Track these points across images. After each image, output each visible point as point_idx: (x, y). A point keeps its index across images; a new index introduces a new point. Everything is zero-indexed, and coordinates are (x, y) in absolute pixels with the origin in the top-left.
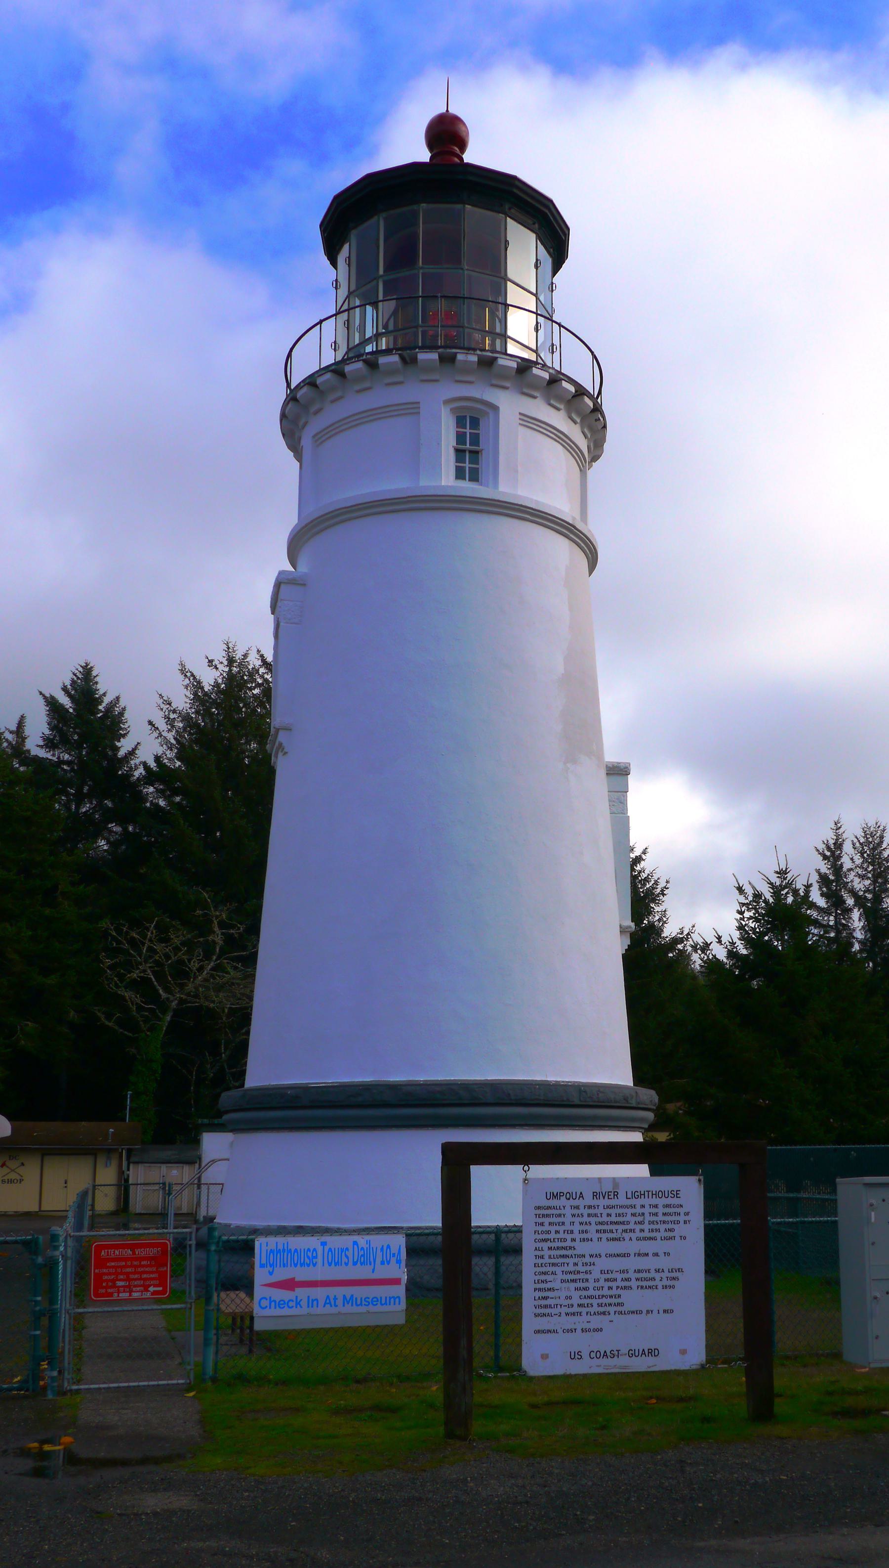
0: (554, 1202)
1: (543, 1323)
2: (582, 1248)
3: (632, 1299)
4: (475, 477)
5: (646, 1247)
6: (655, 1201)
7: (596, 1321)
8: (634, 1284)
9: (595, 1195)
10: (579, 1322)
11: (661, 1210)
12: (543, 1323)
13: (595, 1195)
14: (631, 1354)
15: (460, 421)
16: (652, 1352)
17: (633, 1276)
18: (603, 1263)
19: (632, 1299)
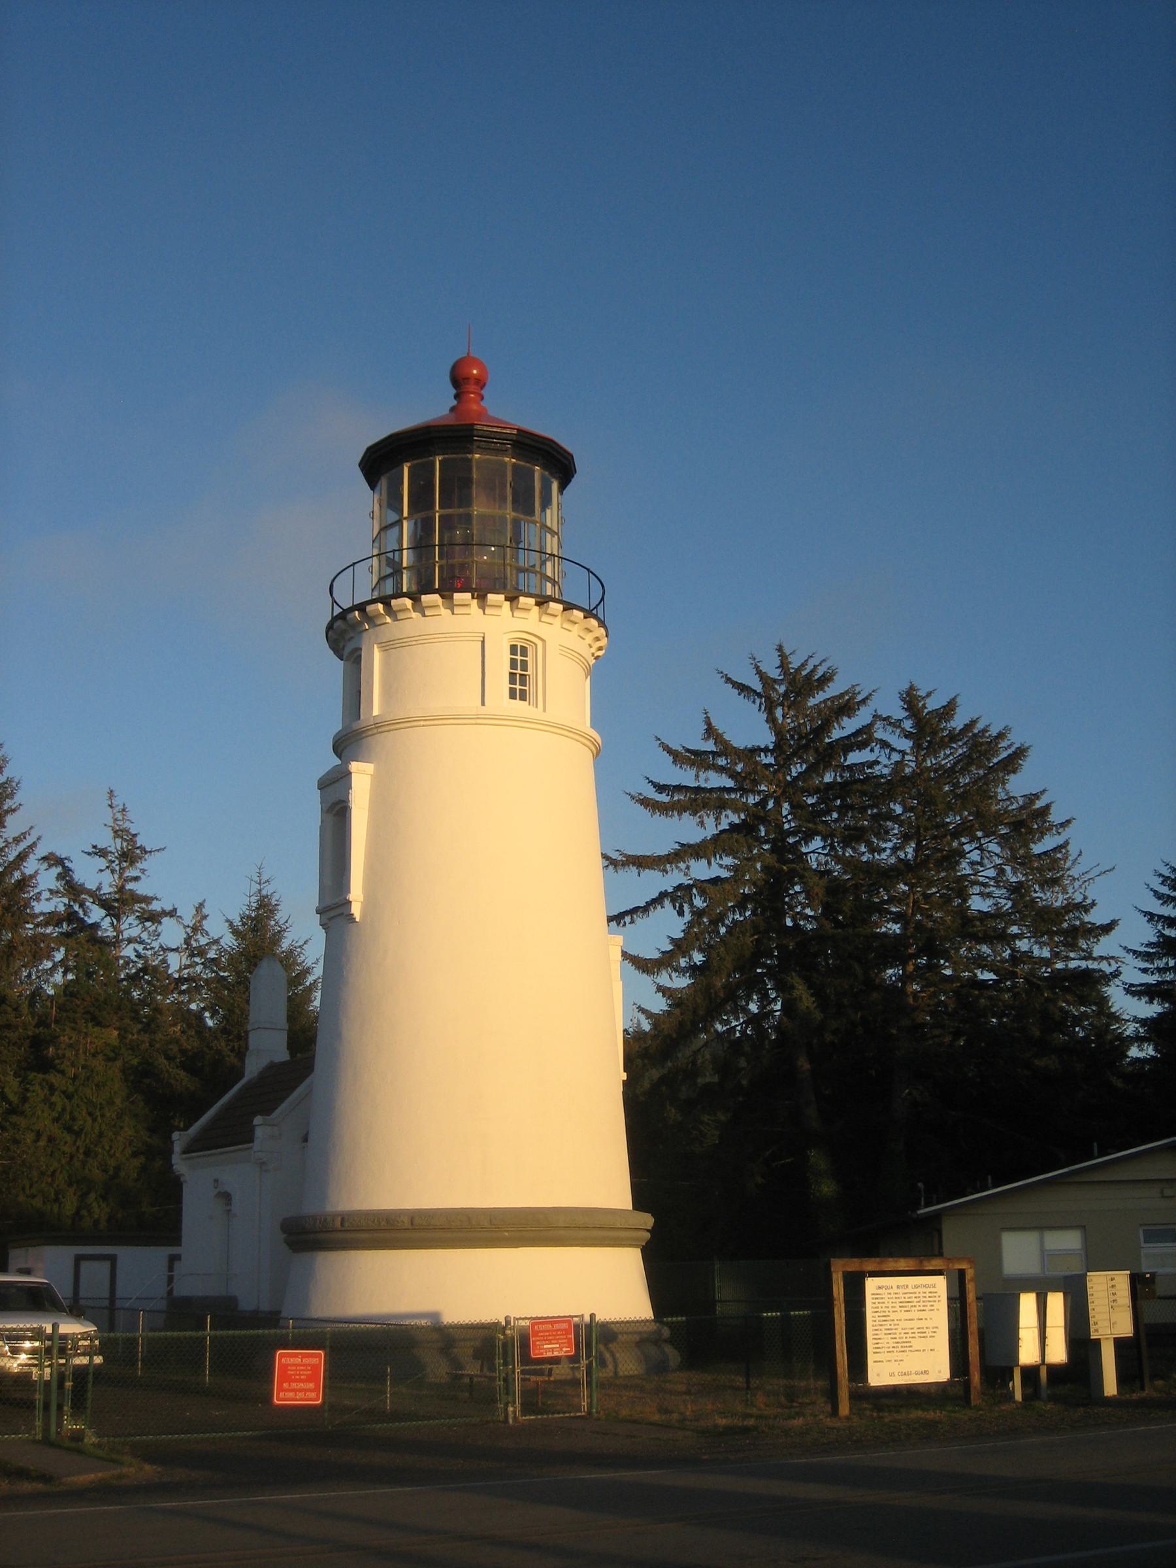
0: (880, 1291)
1: (878, 1357)
2: (893, 1316)
3: (917, 1344)
4: (523, 697)
5: (922, 1315)
6: (924, 1290)
7: (901, 1356)
8: (916, 1335)
9: (898, 1287)
10: (893, 1356)
11: (928, 1295)
12: (878, 1357)
13: (898, 1287)
14: (917, 1374)
15: (513, 650)
16: (926, 1372)
17: (915, 1330)
18: (903, 1324)
19: (917, 1344)
